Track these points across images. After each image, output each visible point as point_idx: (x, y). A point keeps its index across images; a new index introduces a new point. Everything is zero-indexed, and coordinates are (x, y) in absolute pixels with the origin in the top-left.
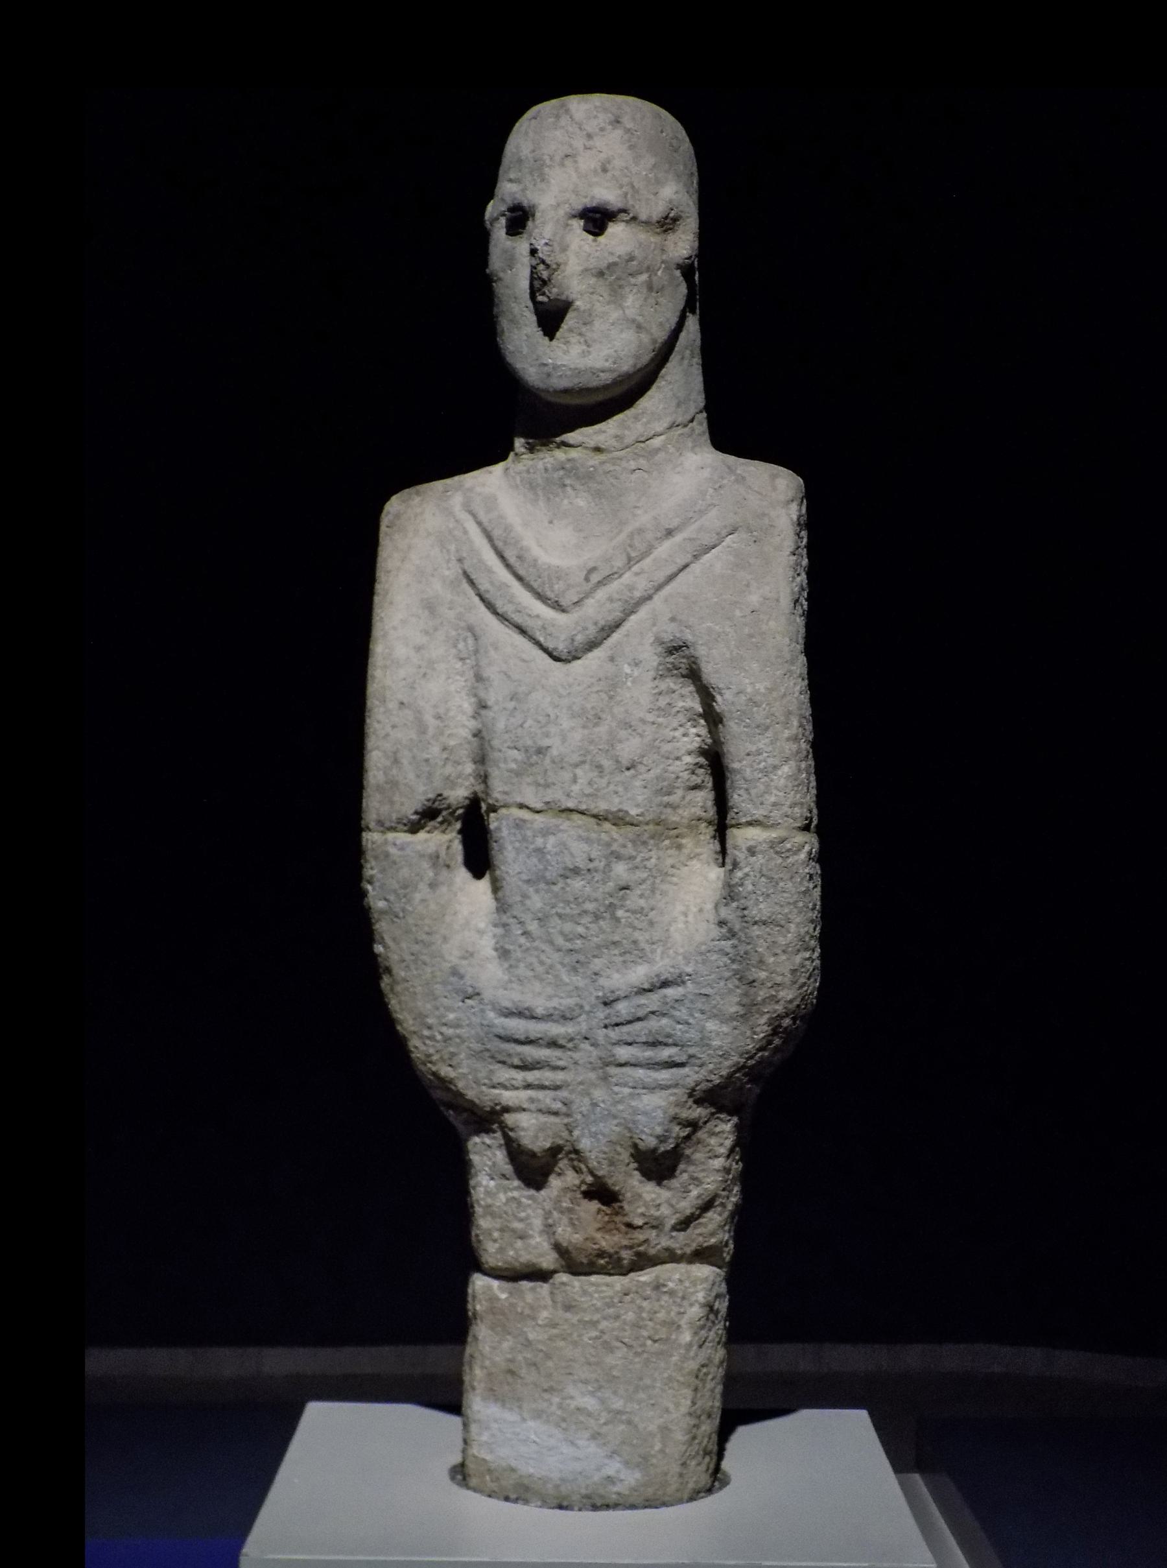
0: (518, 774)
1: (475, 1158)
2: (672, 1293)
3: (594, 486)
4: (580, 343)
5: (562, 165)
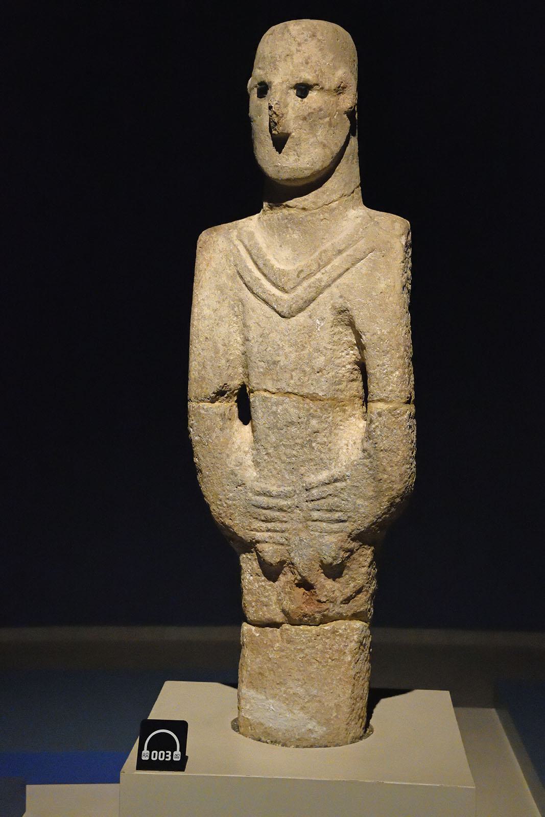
0: (264, 374)
2: (341, 635)
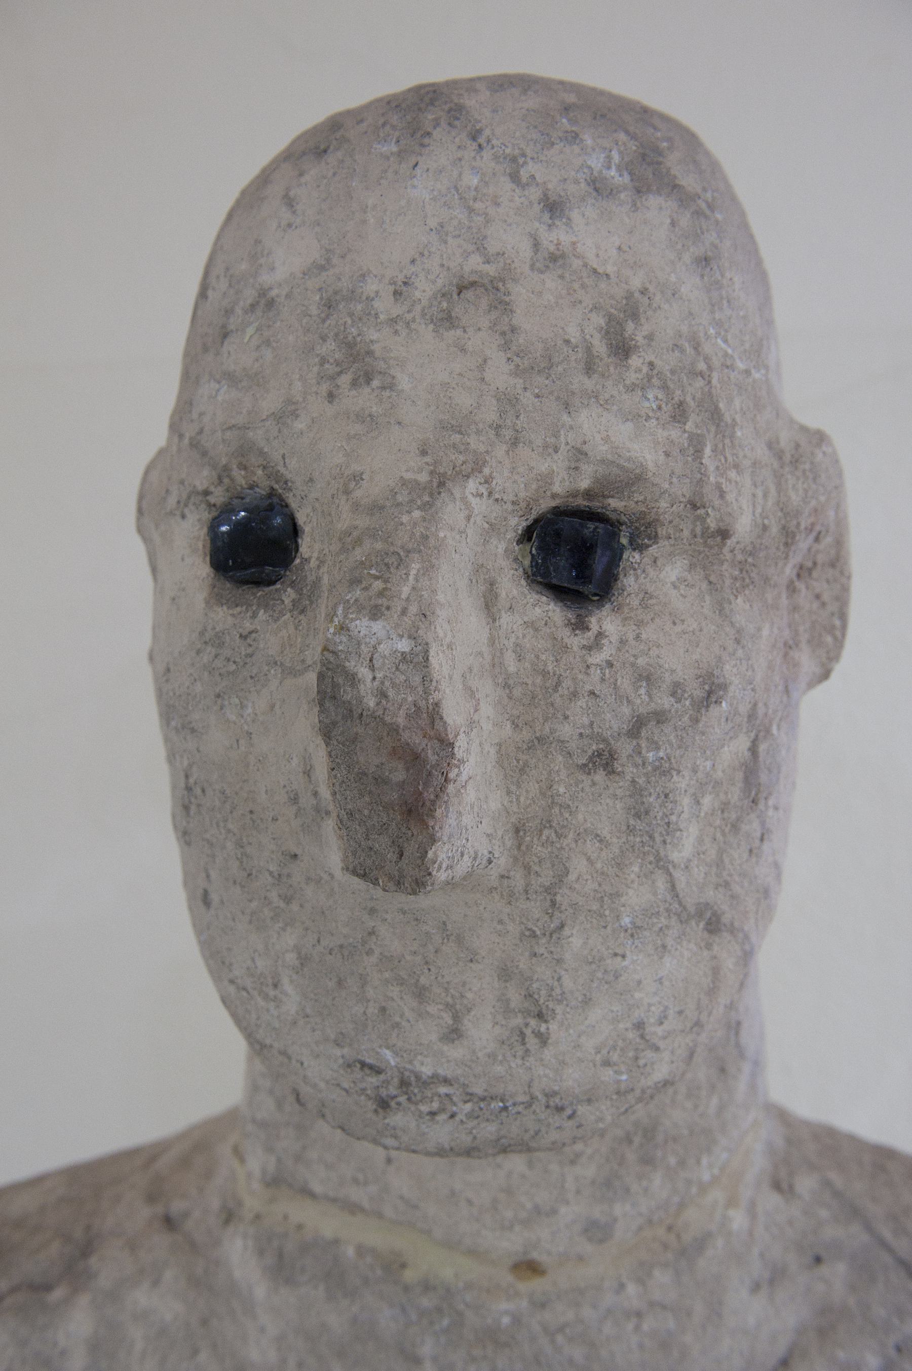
5: (448, 320)
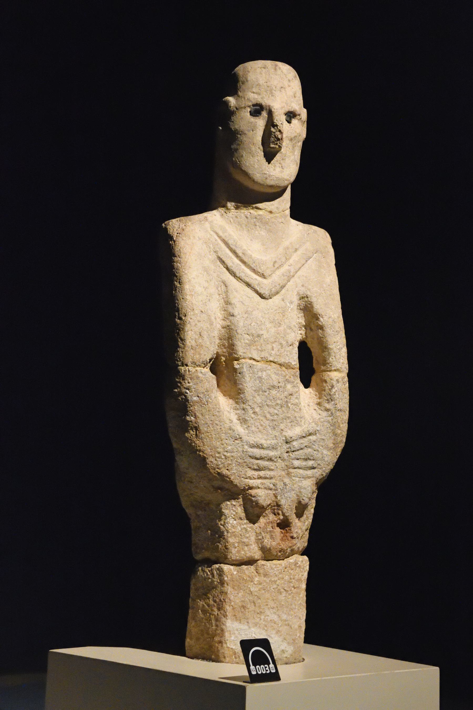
1: (226, 511)
2: (300, 567)
3: (268, 227)
4: (280, 167)
